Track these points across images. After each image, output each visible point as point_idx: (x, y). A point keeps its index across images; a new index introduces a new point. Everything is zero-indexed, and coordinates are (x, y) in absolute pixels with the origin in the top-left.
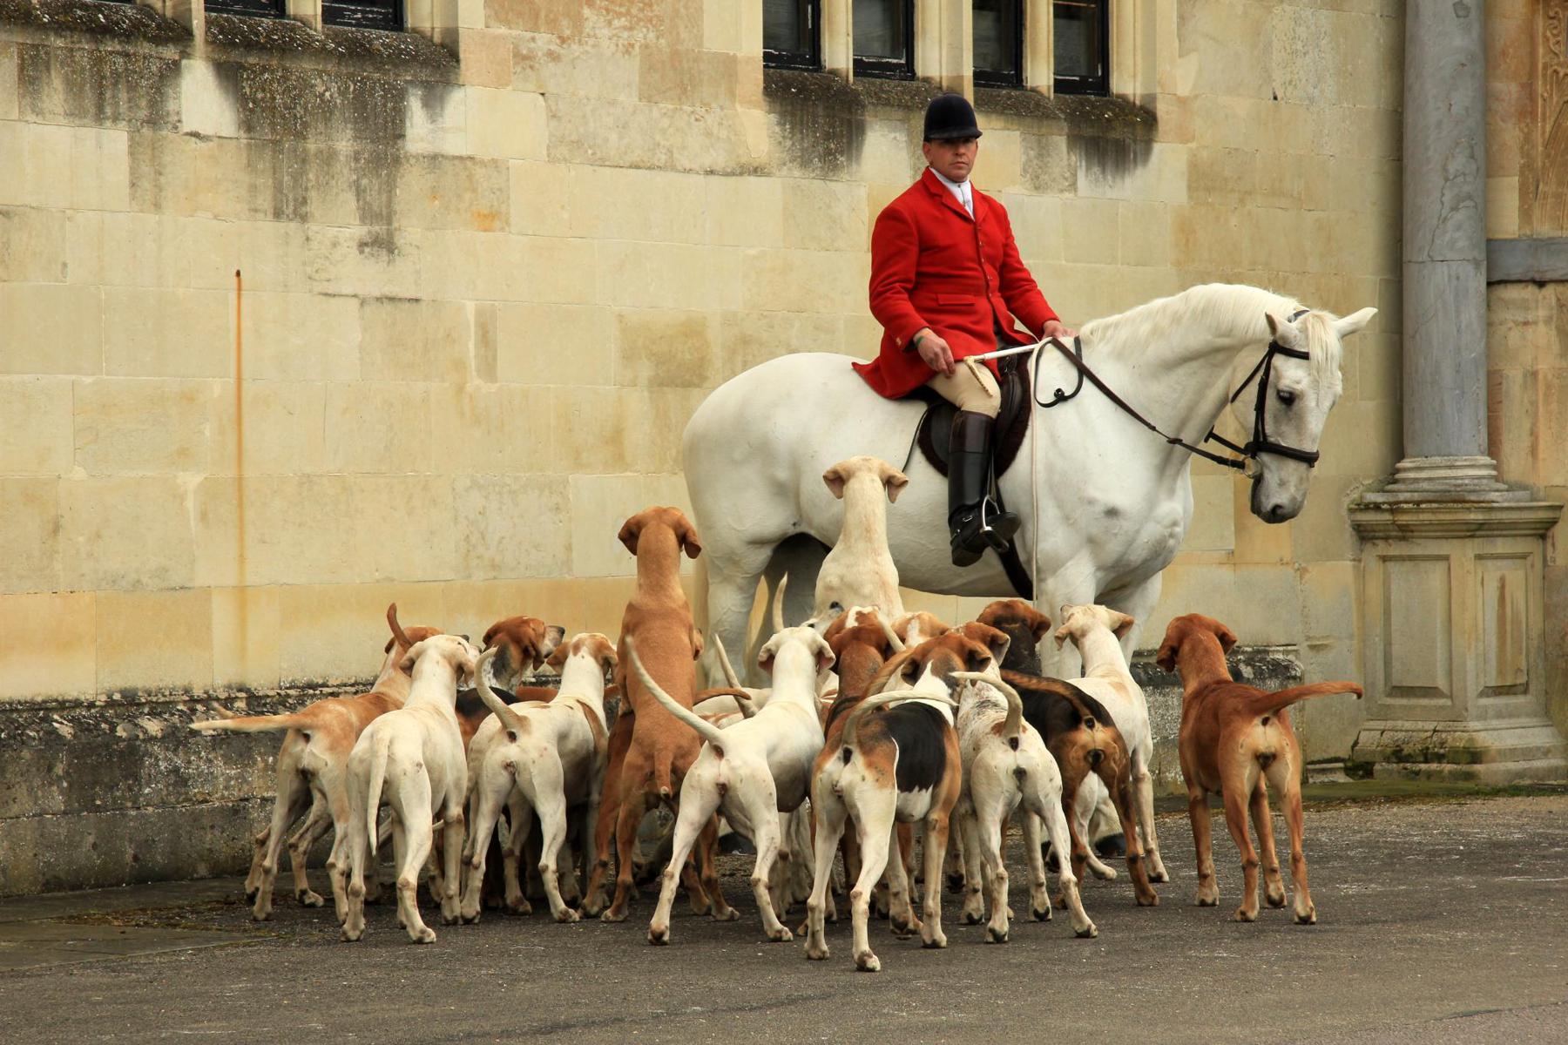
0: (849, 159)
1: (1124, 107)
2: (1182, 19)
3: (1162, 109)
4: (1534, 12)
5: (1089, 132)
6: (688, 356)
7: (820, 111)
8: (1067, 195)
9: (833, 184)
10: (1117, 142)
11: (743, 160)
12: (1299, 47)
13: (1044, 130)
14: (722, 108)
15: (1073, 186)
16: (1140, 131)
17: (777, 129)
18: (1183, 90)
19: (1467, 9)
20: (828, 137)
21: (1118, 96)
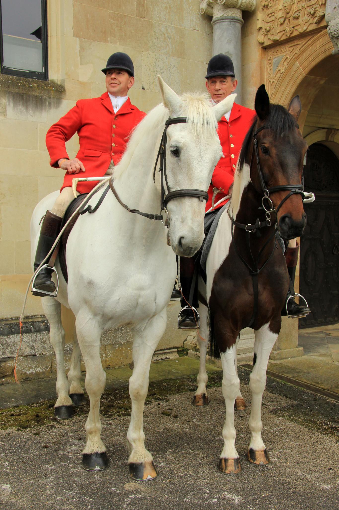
1: (54, 84)
2: (82, 49)
3: (68, 86)
5: (17, 90)
10: (36, 97)
12: (159, 69)
16: (52, 94)
18: (83, 79)
21: (51, 81)
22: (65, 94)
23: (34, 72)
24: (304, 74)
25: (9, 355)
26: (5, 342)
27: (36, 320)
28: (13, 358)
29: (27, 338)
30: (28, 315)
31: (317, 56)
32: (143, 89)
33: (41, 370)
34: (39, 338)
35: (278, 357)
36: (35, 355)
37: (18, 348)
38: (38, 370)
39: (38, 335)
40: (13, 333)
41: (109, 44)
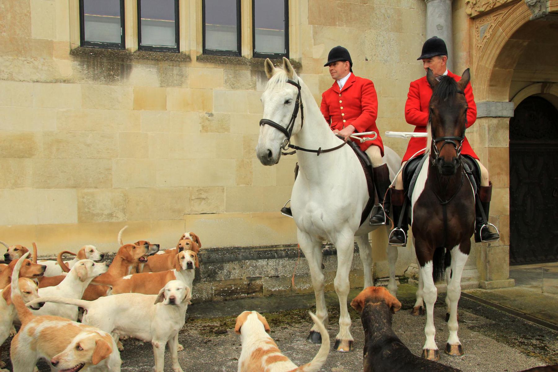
0: (122, 77)
2: (315, 33)
3: (304, 63)
4: (470, 27)
6: (22, 147)
7: (105, 60)
8: (250, 90)
9: (112, 86)
11: (57, 78)
13: (237, 68)
14: (44, 59)
15: (254, 87)
17: (78, 67)
19: (442, 27)
20: (109, 70)
22: (302, 69)
23: (278, 54)
24: (507, 39)
25: (258, 275)
26: (255, 265)
27: (279, 249)
28: (261, 277)
29: (272, 262)
30: (273, 244)
31: (518, 23)
32: (367, 60)
33: (283, 289)
34: (281, 263)
35: (490, 286)
36: (278, 277)
37: (265, 270)
38: (281, 288)
39: (281, 260)
40: (260, 258)
41: (337, 27)
